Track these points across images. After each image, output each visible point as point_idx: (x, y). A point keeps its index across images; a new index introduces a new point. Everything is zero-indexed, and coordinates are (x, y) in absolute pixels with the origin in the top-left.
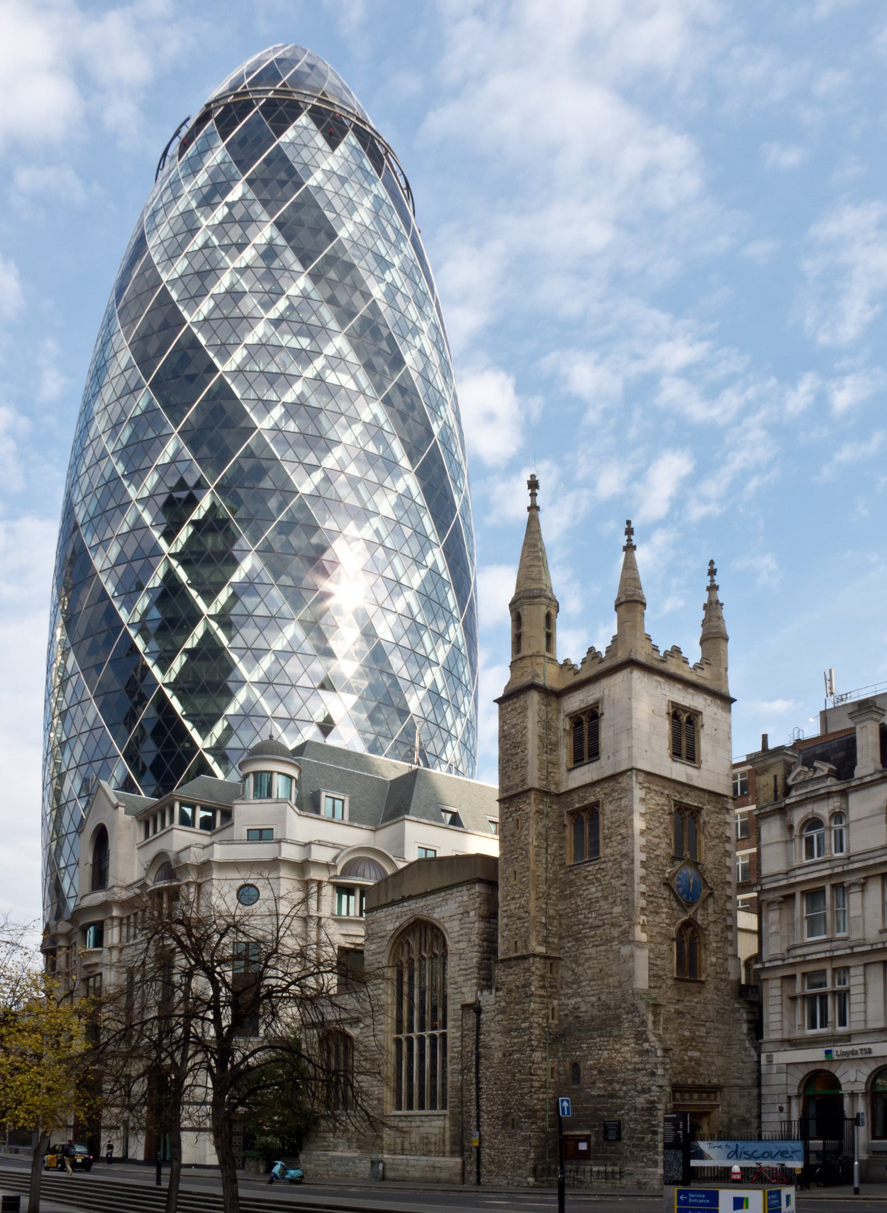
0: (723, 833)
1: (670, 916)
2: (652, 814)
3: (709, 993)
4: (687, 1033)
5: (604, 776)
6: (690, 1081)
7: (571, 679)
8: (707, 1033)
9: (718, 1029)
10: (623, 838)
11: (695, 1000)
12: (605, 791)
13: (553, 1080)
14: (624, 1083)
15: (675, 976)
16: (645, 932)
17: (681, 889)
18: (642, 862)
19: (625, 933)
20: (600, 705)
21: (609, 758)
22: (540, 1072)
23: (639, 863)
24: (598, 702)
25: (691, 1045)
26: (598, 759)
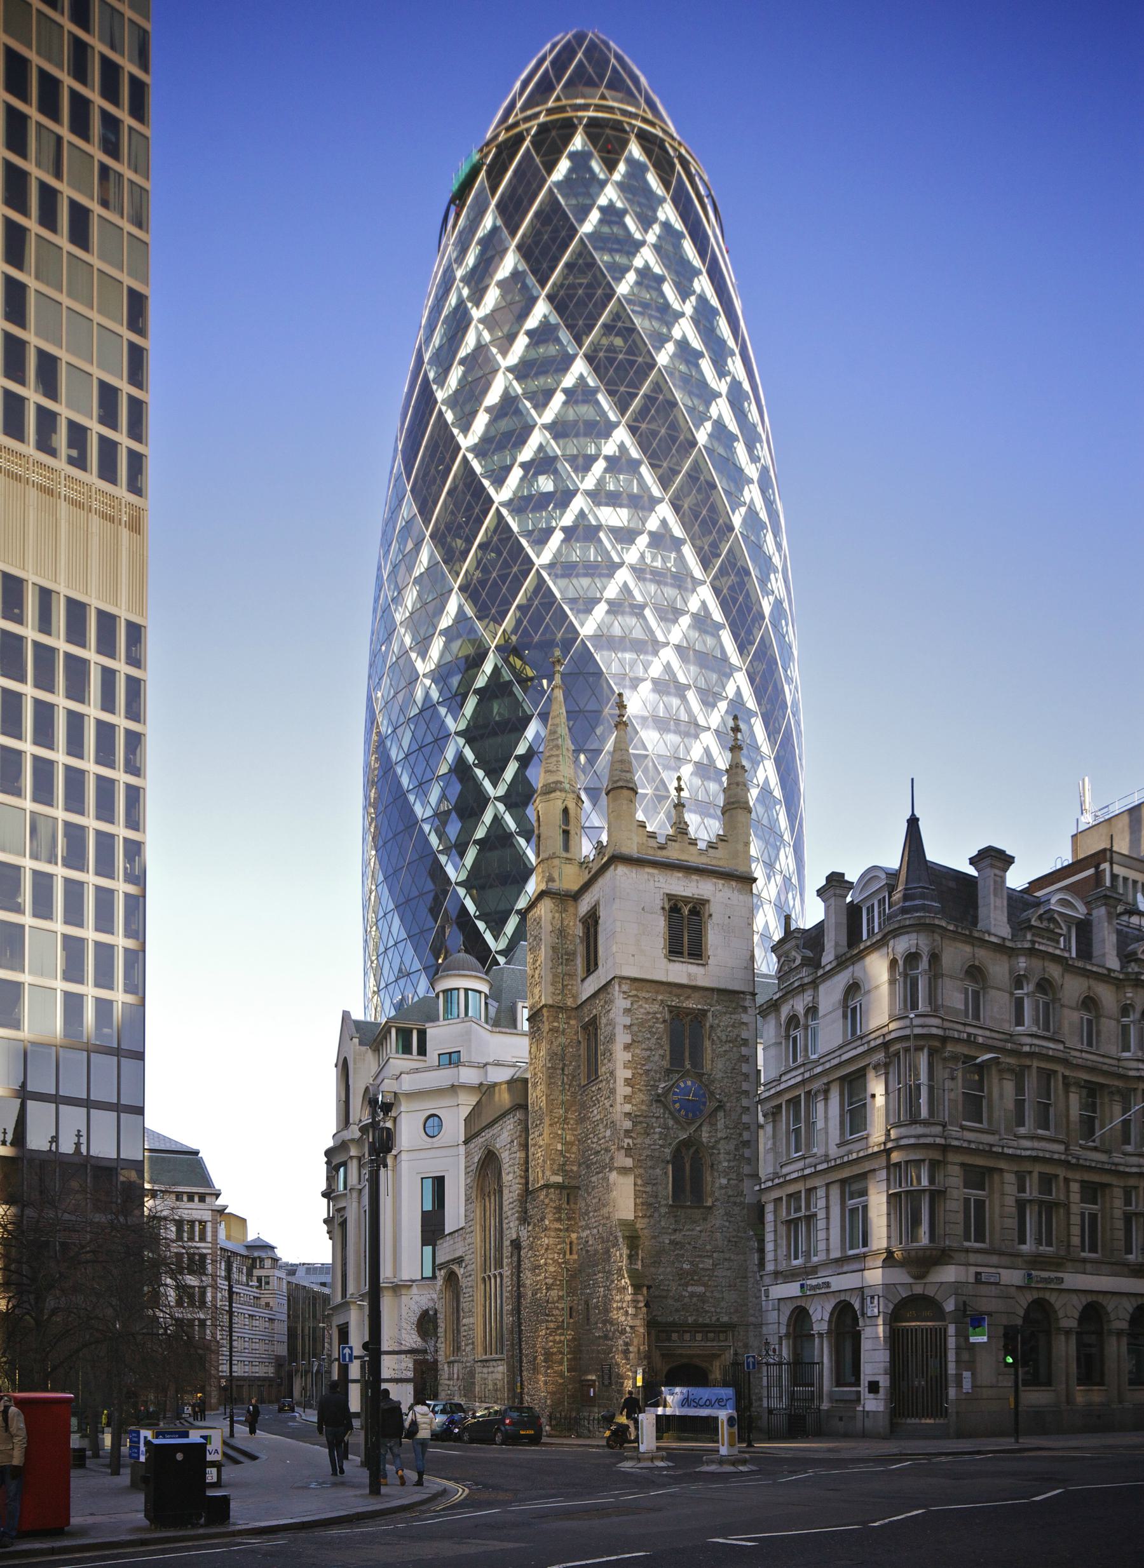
0: (738, 1036)
1: (664, 1137)
2: (641, 1024)
3: (717, 1220)
4: (686, 1266)
9: (729, 1260)
11: (698, 1228)
13: (572, 1321)
15: (671, 1203)
16: (631, 1156)
17: (677, 1105)
18: (626, 1080)
19: (612, 1158)
22: (555, 1312)
23: (623, 1080)
25: (692, 1279)
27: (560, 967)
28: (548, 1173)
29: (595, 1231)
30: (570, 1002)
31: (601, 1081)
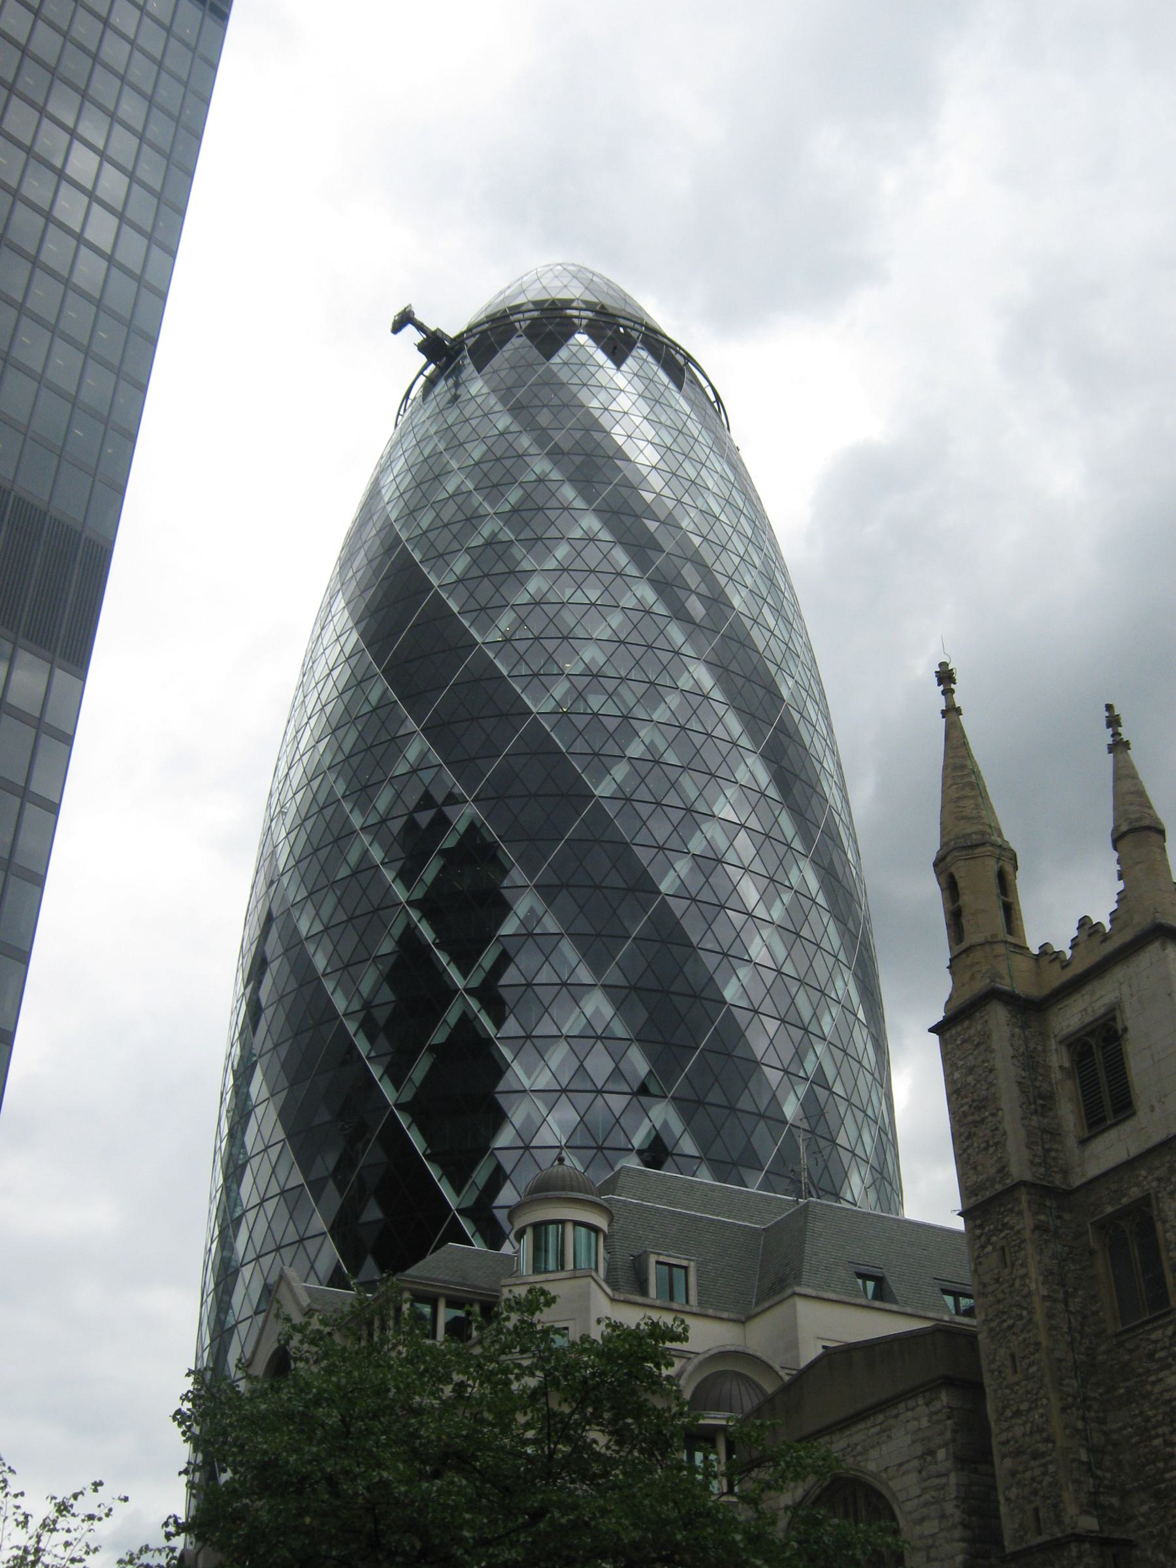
5: (1149, 1145)
7: (1055, 978)
12: (1157, 1174)
20: (1118, 1014)
21: (1152, 1109)
24: (1114, 1009)
26: (1134, 1114)
27: (1034, 1118)
28: (1071, 1510)
30: (1058, 1180)
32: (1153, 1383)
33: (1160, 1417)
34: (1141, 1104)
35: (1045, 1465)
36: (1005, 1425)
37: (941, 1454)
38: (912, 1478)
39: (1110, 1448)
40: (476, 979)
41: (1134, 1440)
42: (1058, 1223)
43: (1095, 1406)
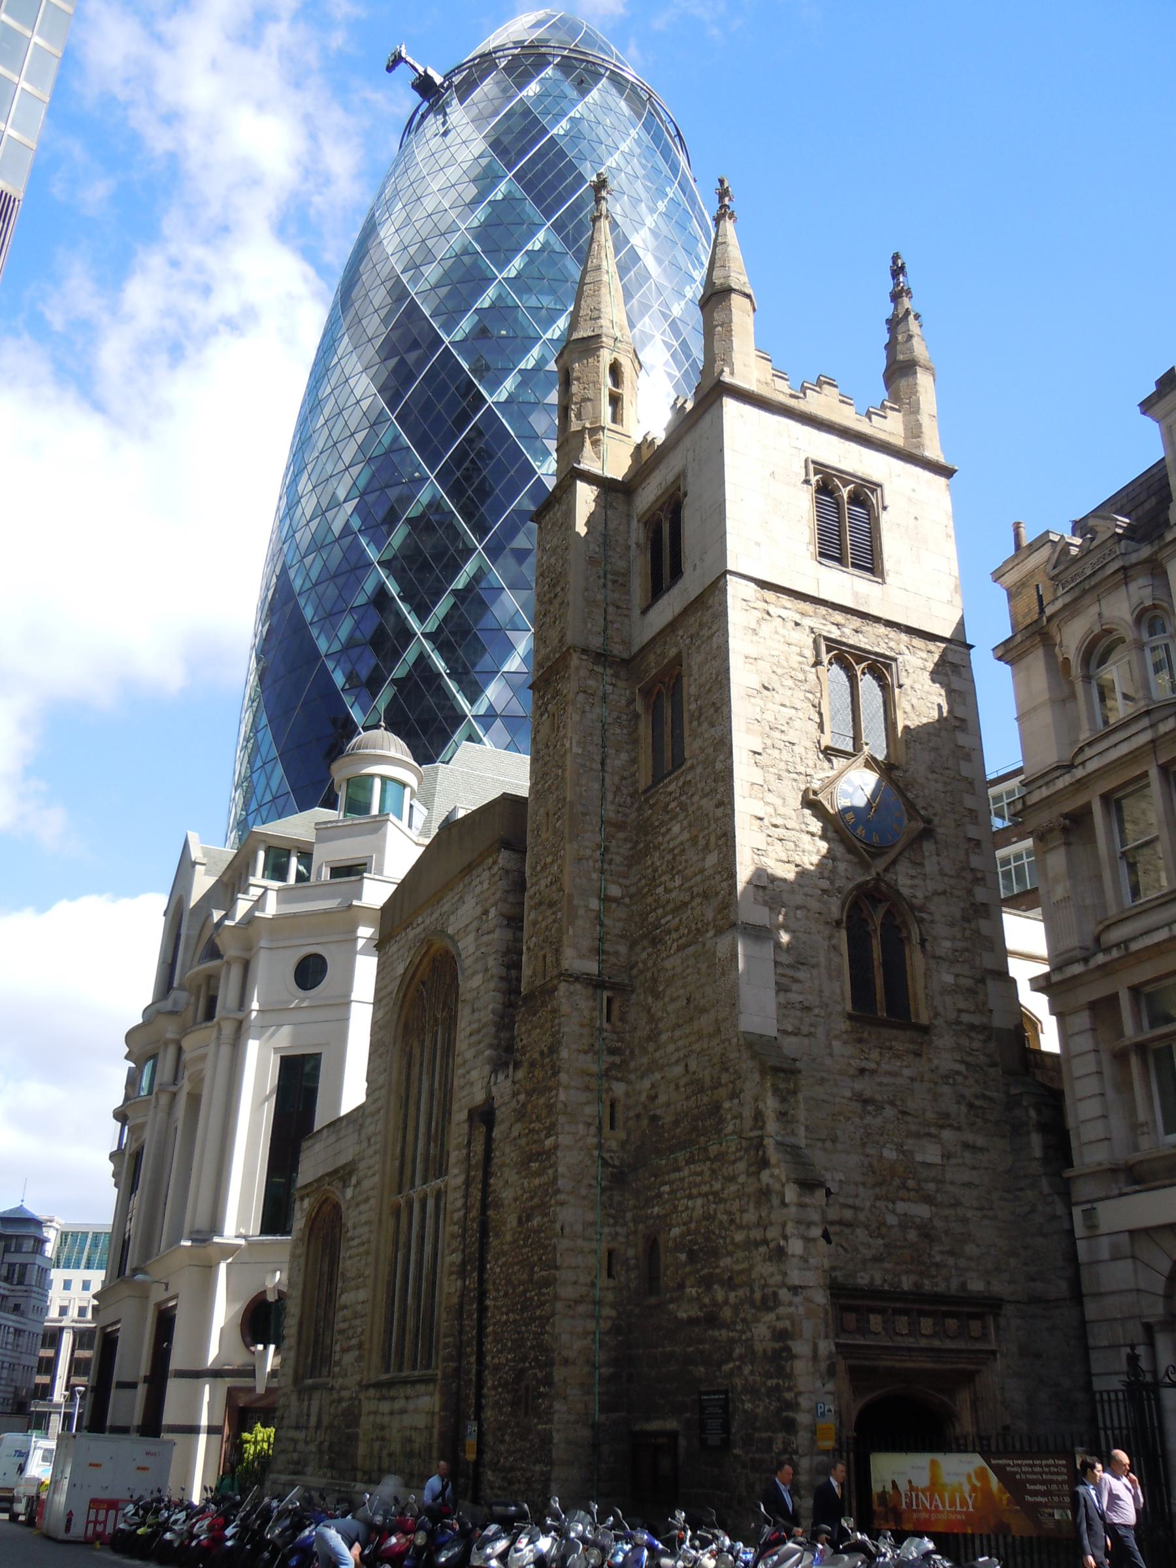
6: (906, 1283)
8: (947, 1156)
10: (716, 711)
12: (693, 630)
14: (730, 1284)
24: (678, 477)
29: (679, 1070)
30: (617, 650)
31: (692, 767)
32: (664, 835)
33: (664, 867)
34: (687, 567)
35: (554, 913)
36: (535, 879)
37: (493, 912)
38: (471, 938)
39: (627, 900)
40: (431, 625)
41: (646, 889)
42: (609, 689)
43: (618, 859)
